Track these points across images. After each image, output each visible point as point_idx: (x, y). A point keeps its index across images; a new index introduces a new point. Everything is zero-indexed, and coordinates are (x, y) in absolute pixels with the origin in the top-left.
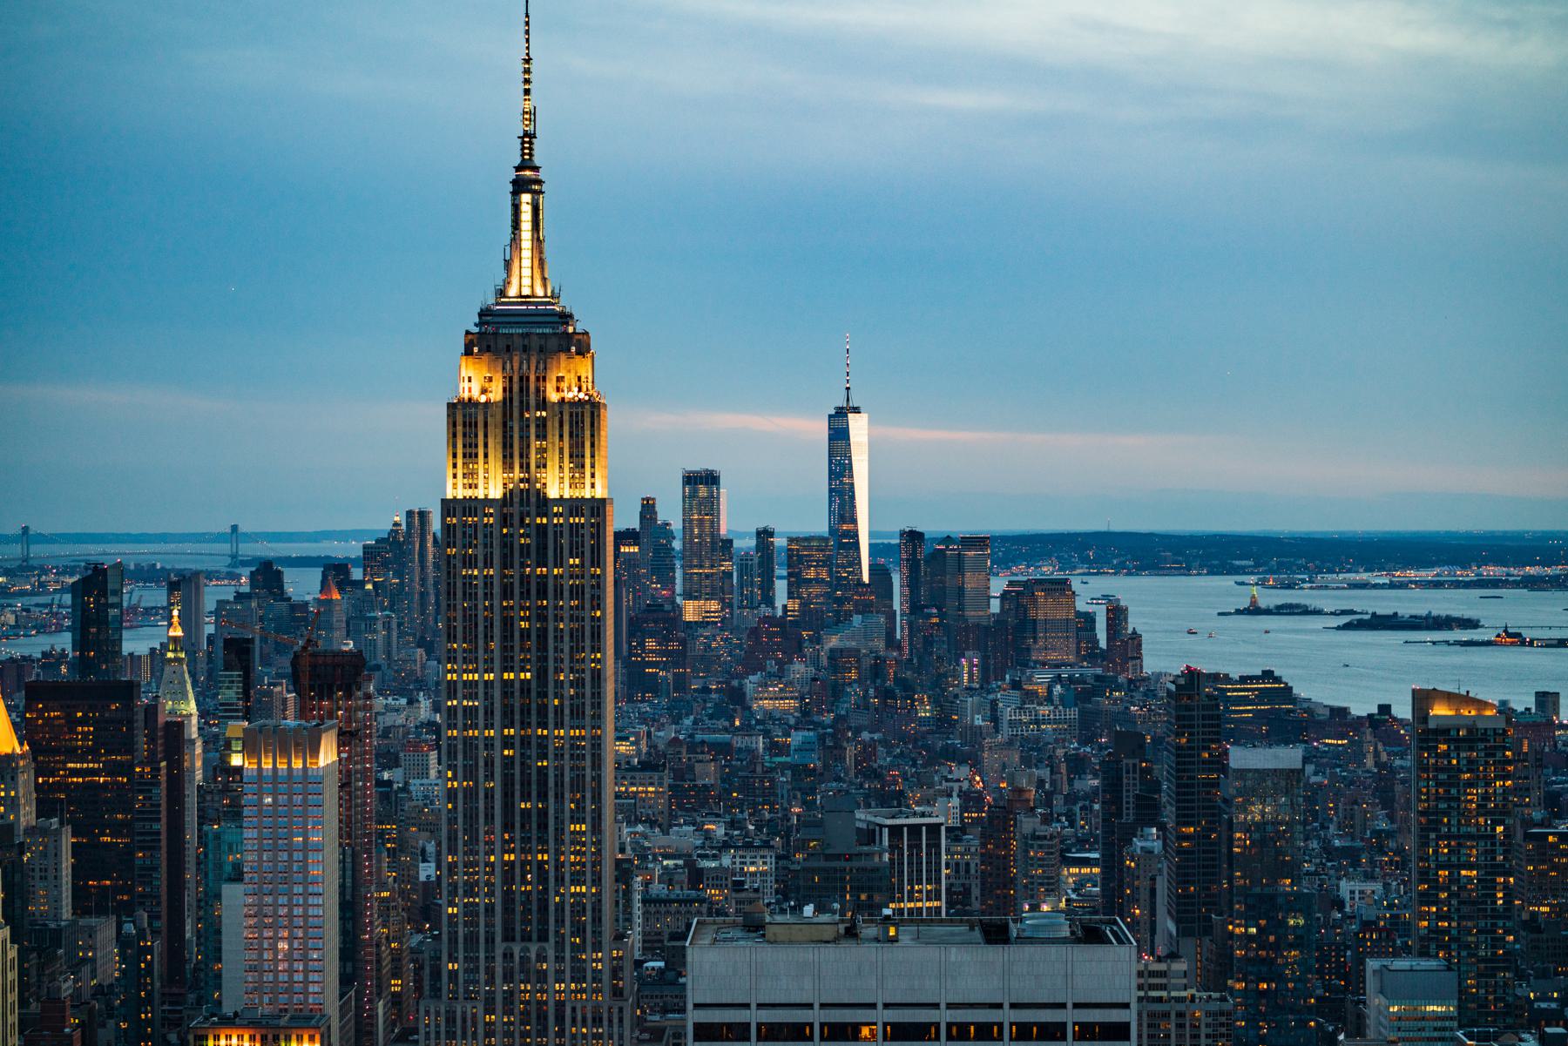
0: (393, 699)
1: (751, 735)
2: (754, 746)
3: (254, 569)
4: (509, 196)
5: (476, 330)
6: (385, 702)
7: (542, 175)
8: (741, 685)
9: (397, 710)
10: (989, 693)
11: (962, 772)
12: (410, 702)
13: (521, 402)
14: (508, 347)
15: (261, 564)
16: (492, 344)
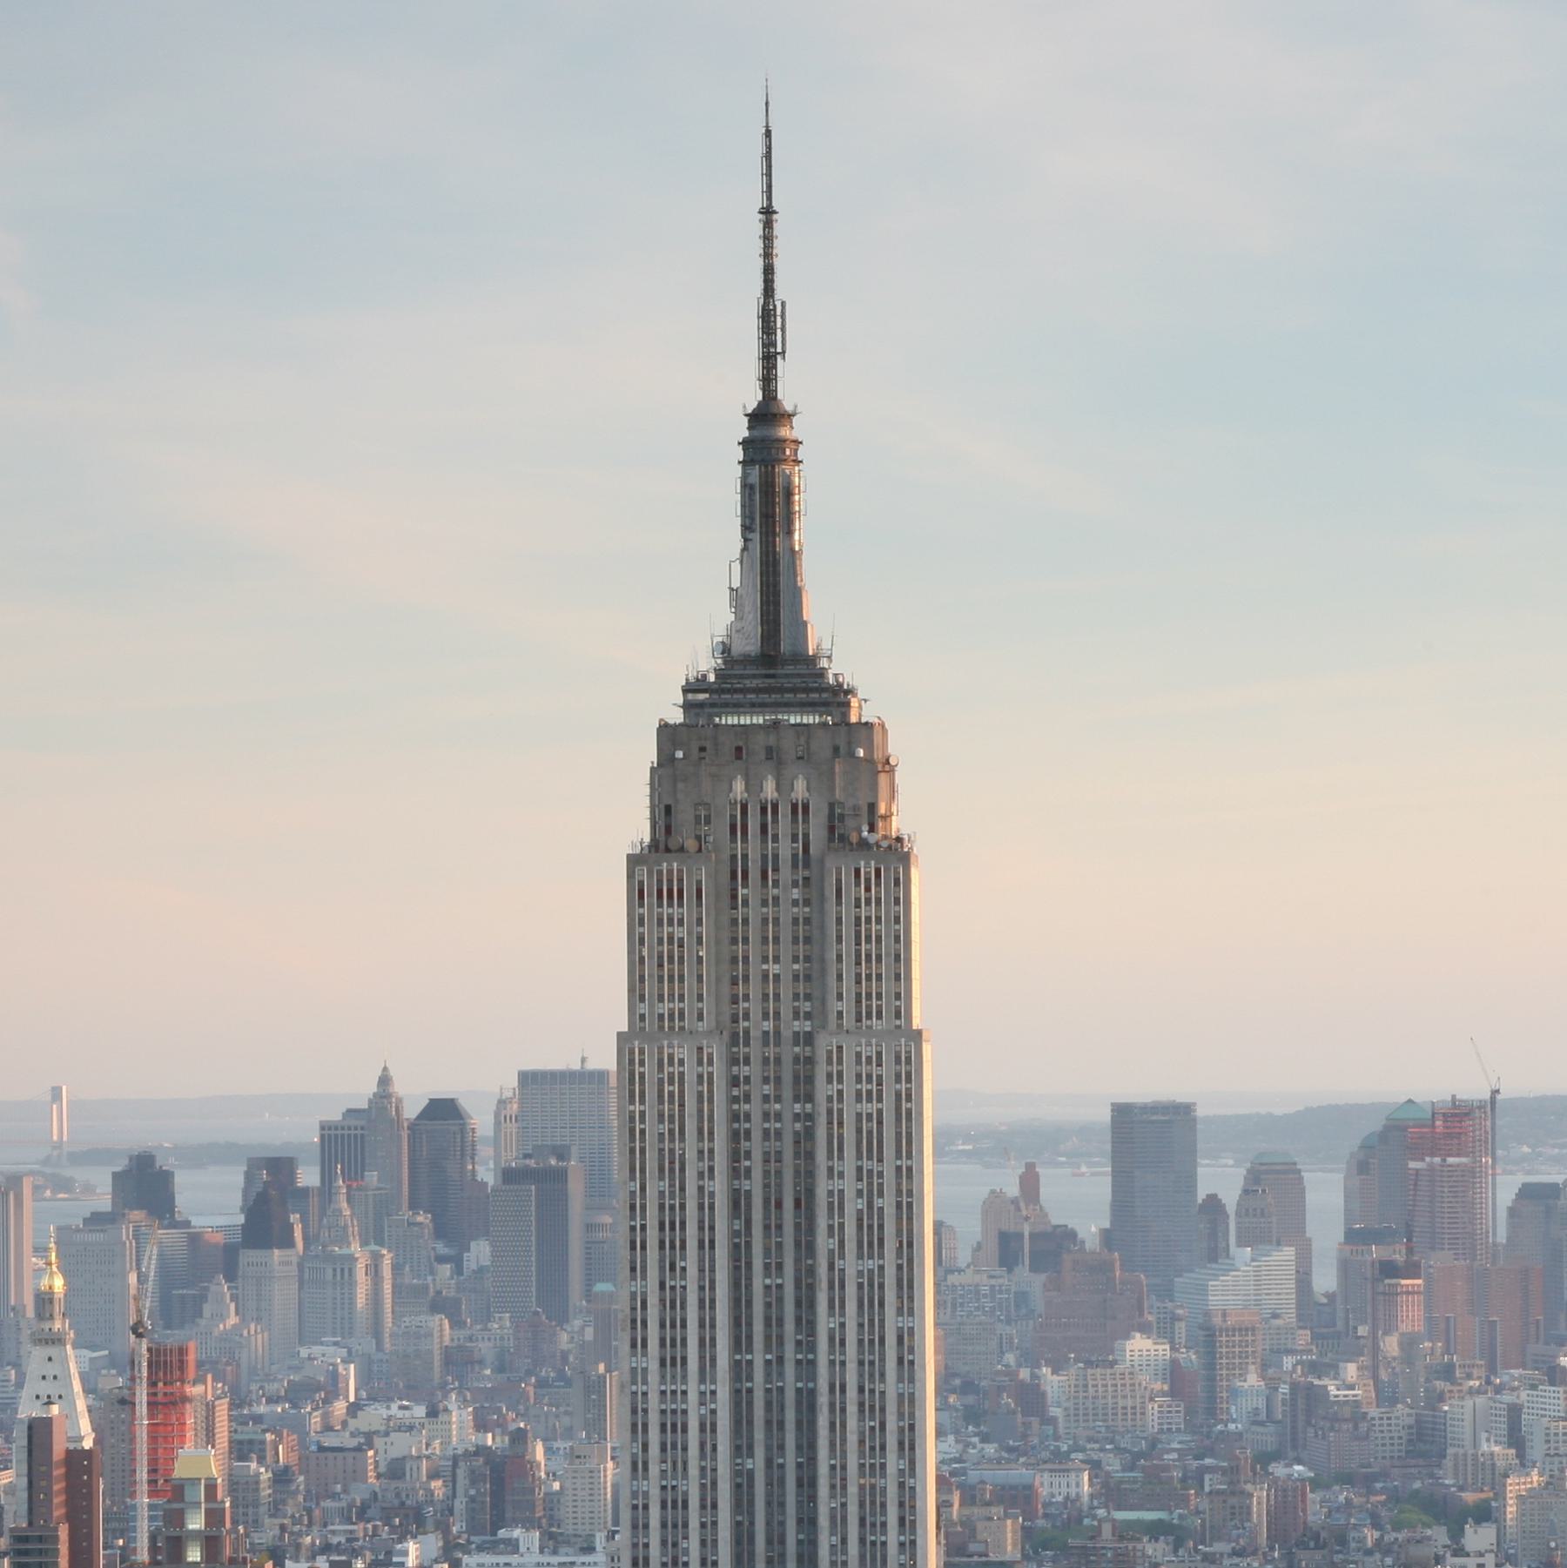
0: (402, 1408)
1: (1068, 1471)
2: (1073, 1491)
3: (118, 1169)
4: (739, 470)
5: (676, 716)
6: (384, 1413)
7: (797, 429)
8: (1034, 1376)
9: (411, 1428)
10: (1499, 1390)
11: (1479, 1538)
12: (433, 1413)
13: (764, 857)
14: (739, 749)
15: (131, 1159)
16: (708, 745)
